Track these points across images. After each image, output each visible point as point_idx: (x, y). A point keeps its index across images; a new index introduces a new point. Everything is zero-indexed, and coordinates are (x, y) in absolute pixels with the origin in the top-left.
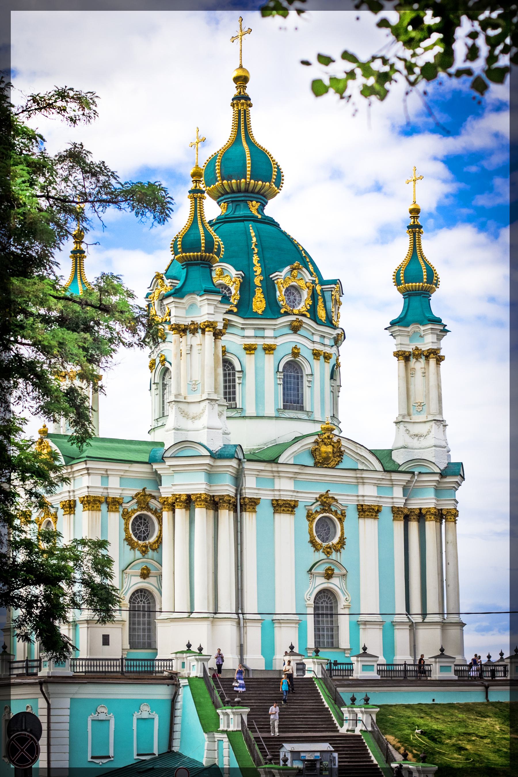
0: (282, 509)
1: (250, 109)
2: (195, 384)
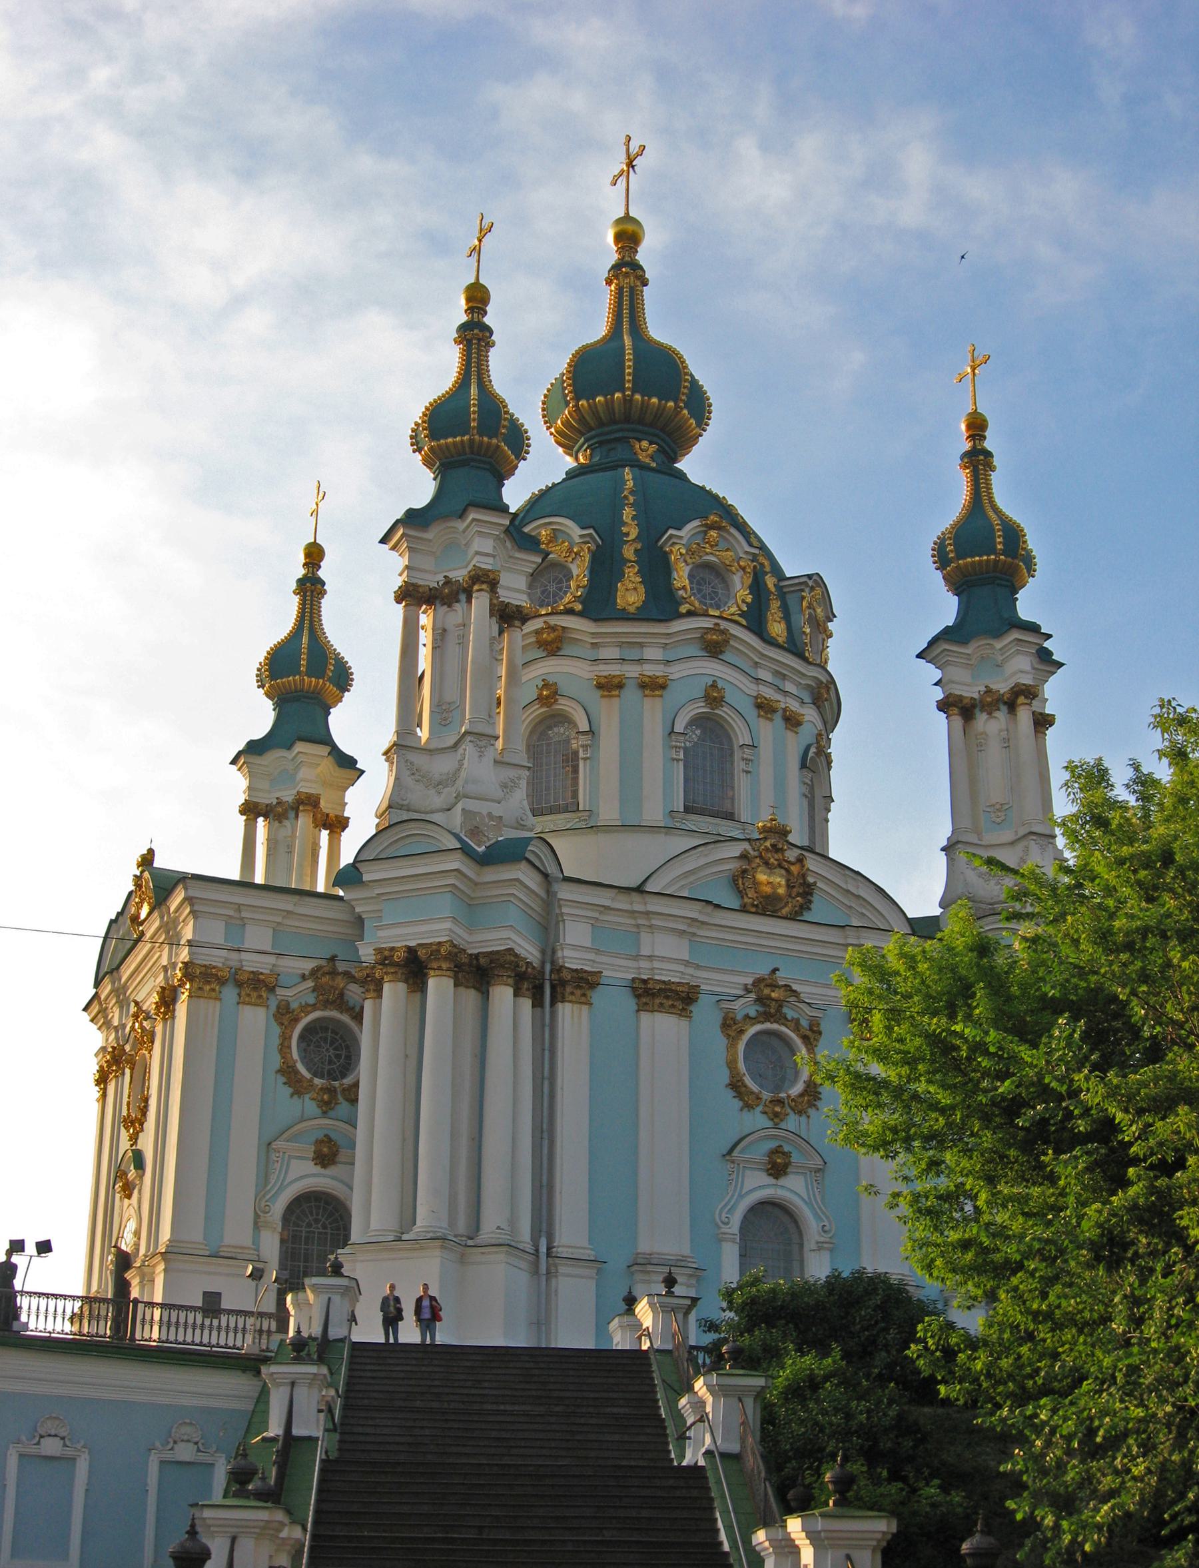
0: (657, 1001)
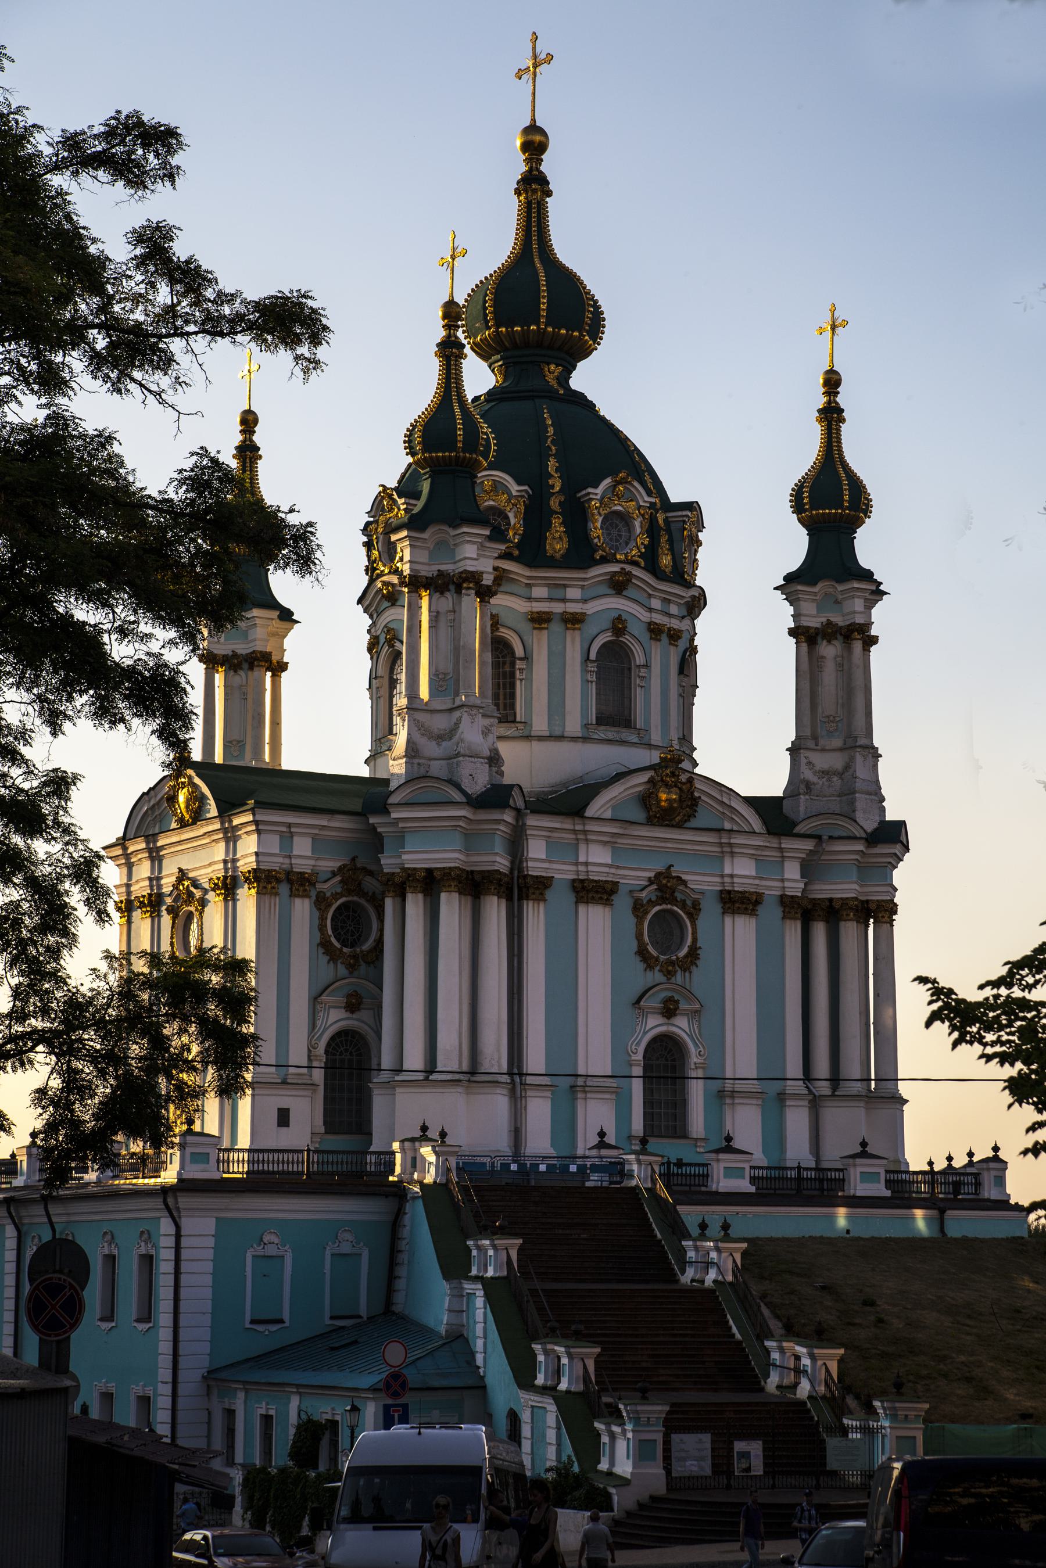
1: (547, 199)
2: (443, 680)
